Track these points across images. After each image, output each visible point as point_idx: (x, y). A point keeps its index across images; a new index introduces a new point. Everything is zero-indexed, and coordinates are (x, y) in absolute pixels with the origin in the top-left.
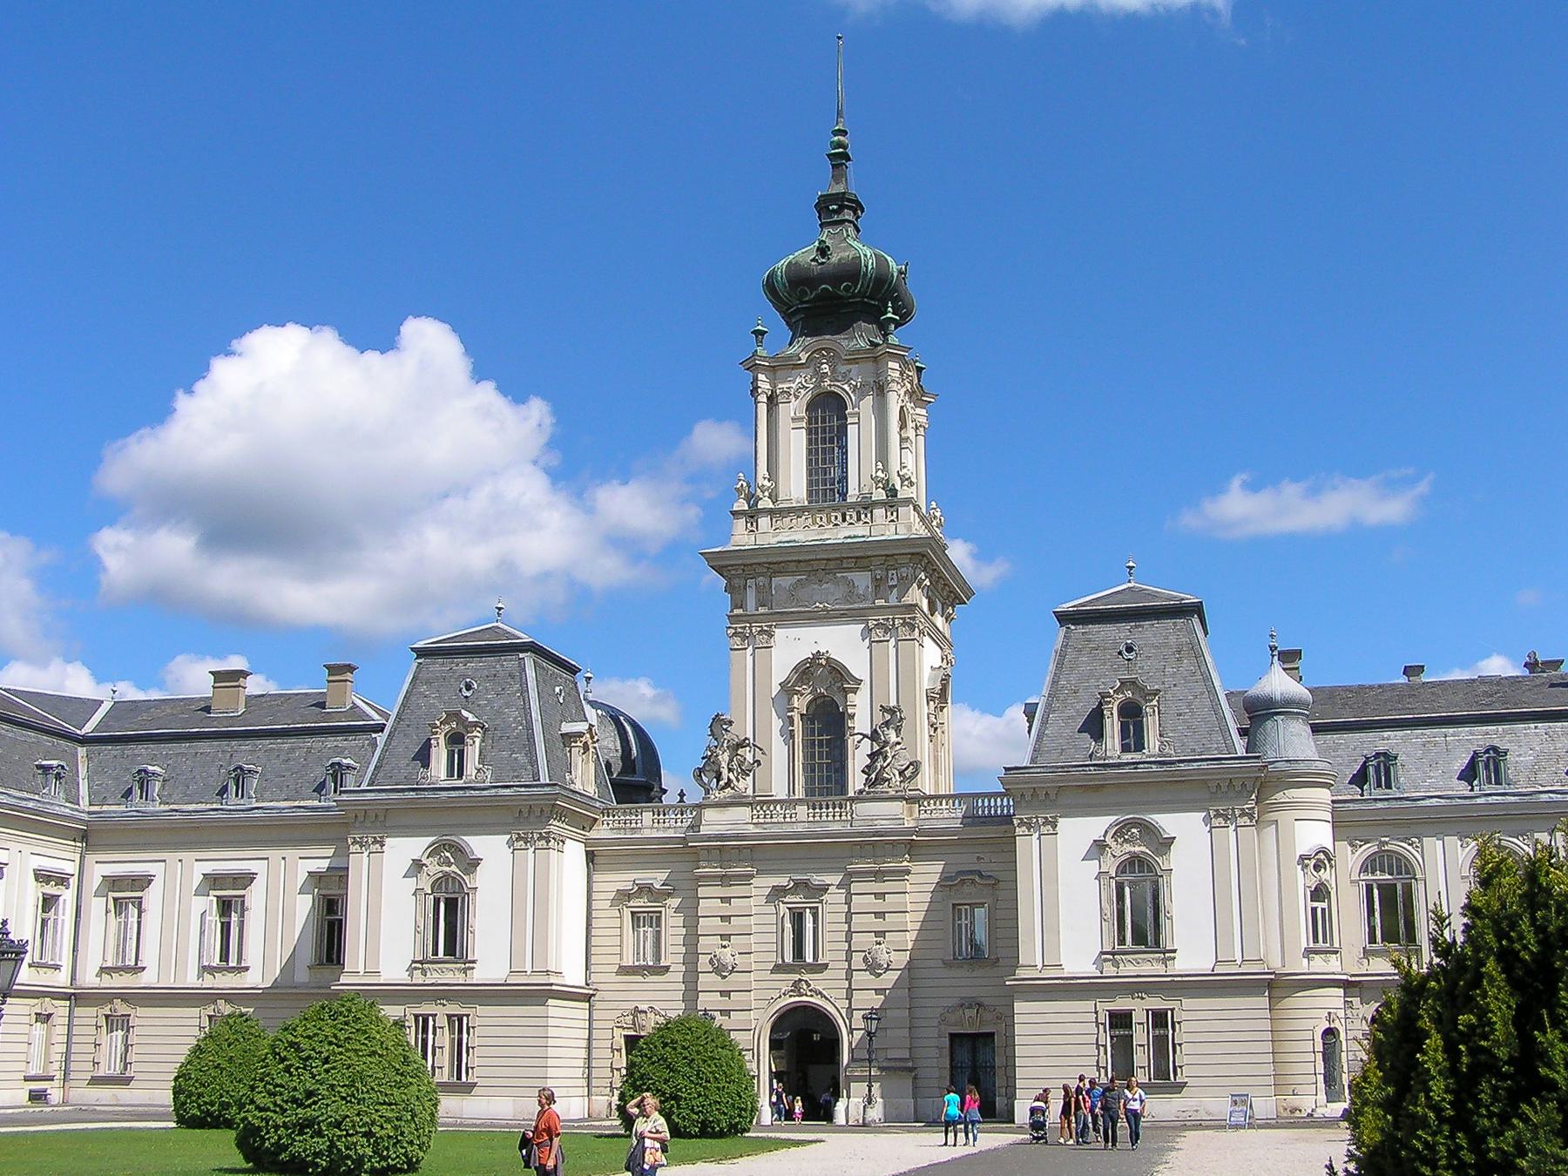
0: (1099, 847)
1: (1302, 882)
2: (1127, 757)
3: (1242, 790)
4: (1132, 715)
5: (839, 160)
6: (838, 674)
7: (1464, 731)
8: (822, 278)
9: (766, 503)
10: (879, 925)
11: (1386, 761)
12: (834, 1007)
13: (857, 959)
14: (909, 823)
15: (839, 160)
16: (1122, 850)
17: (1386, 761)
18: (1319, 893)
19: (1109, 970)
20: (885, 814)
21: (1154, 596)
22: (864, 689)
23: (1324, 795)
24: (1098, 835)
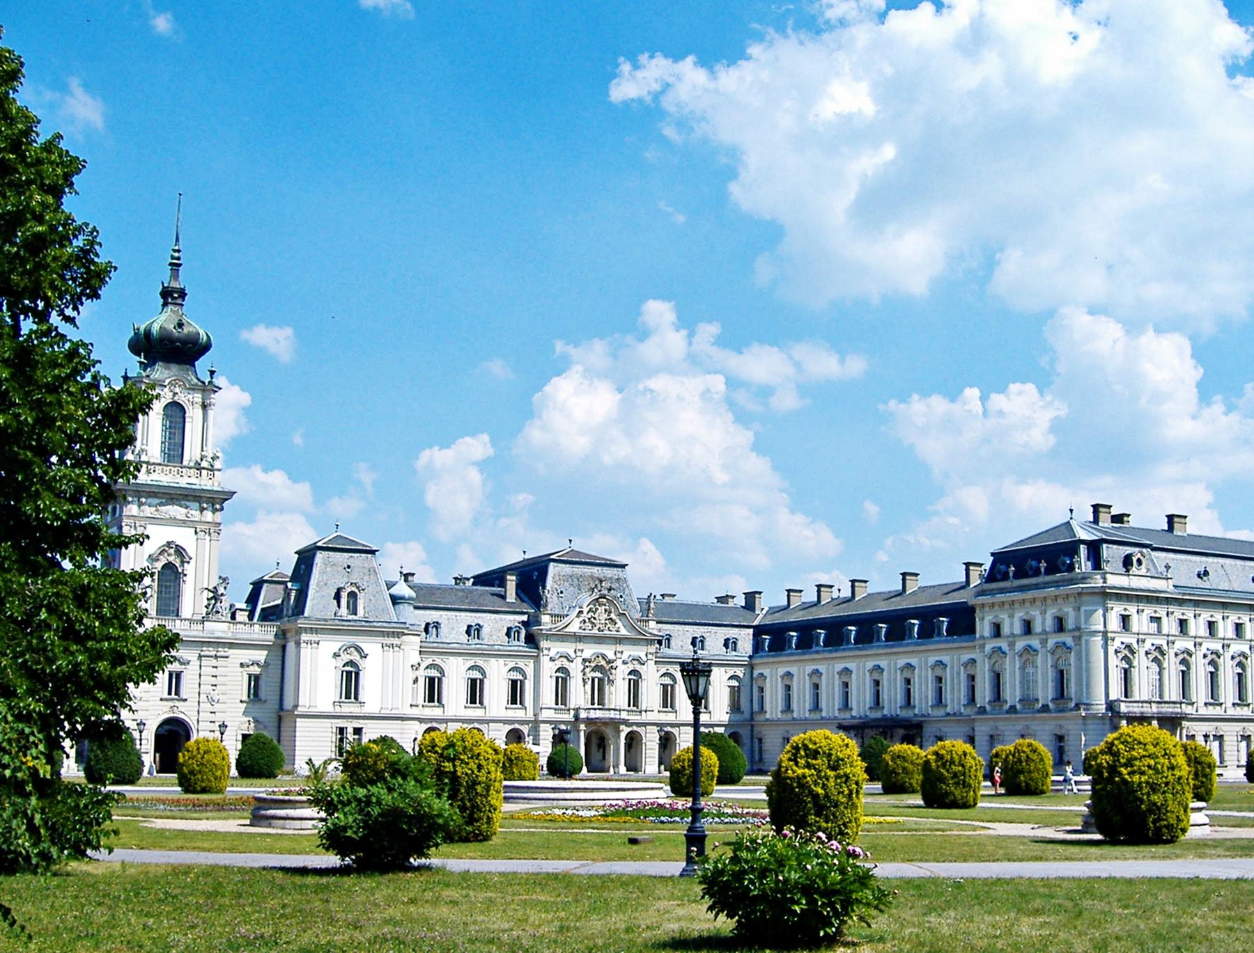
0: (336, 655)
1: (411, 675)
2: (350, 617)
3: (393, 633)
4: (352, 595)
5: (175, 267)
6: (180, 551)
7: (463, 614)
8: (179, 340)
9: (144, 458)
10: (214, 681)
11: (437, 625)
12: (191, 719)
13: (203, 697)
14: (230, 635)
15: (175, 267)
16: (346, 658)
17: (437, 625)
18: (416, 681)
19: (338, 709)
20: (218, 629)
21: (357, 543)
22: (193, 562)
23: (418, 639)
24: (336, 650)
